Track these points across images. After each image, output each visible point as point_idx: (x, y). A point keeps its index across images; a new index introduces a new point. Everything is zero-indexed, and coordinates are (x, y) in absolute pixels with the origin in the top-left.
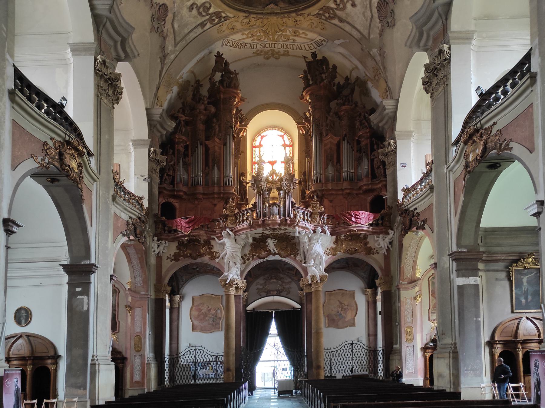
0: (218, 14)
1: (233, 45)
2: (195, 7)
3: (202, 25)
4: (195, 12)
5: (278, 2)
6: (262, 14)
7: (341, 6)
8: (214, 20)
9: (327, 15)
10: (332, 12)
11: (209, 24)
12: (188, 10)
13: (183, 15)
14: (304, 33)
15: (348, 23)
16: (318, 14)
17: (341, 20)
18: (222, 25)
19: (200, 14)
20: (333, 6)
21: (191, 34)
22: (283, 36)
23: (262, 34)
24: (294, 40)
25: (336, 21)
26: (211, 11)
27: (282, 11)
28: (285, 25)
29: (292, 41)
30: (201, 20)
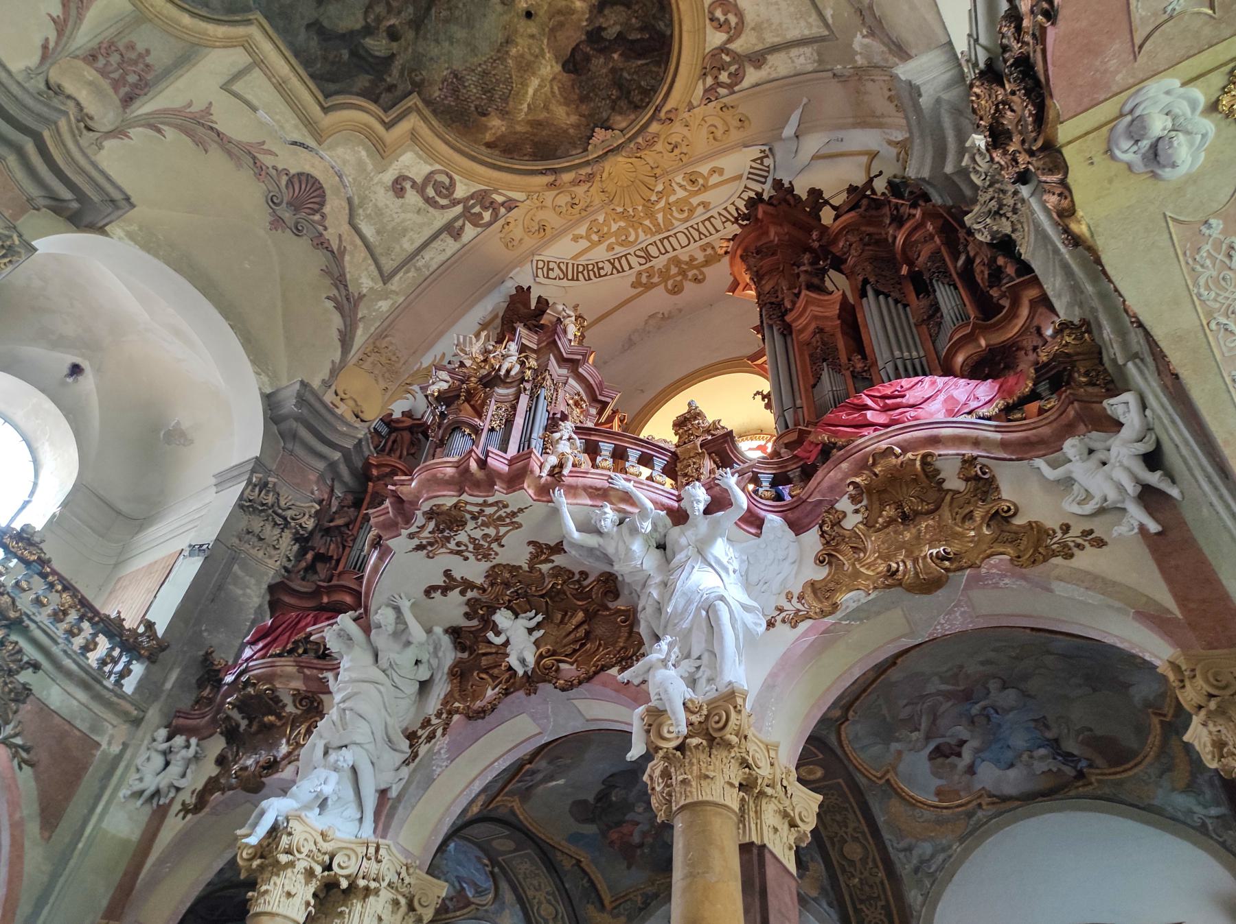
0: (483, 198)
1: (566, 275)
2: (408, 185)
3: (450, 228)
4: (412, 197)
5: (608, 119)
6: (587, 163)
7: (733, 20)
8: (480, 216)
9: (724, 77)
10: (727, 59)
11: (468, 226)
12: (391, 193)
13: (380, 205)
14: (713, 171)
15: (775, 49)
16: (706, 91)
17: (757, 59)
18: (508, 223)
19: (429, 201)
20: (716, 38)
21: (428, 254)
22: (674, 209)
23: (622, 224)
24: (705, 205)
25: (752, 76)
26: (461, 191)
27: (627, 136)
28: (658, 171)
29: (700, 210)
30: (440, 219)
